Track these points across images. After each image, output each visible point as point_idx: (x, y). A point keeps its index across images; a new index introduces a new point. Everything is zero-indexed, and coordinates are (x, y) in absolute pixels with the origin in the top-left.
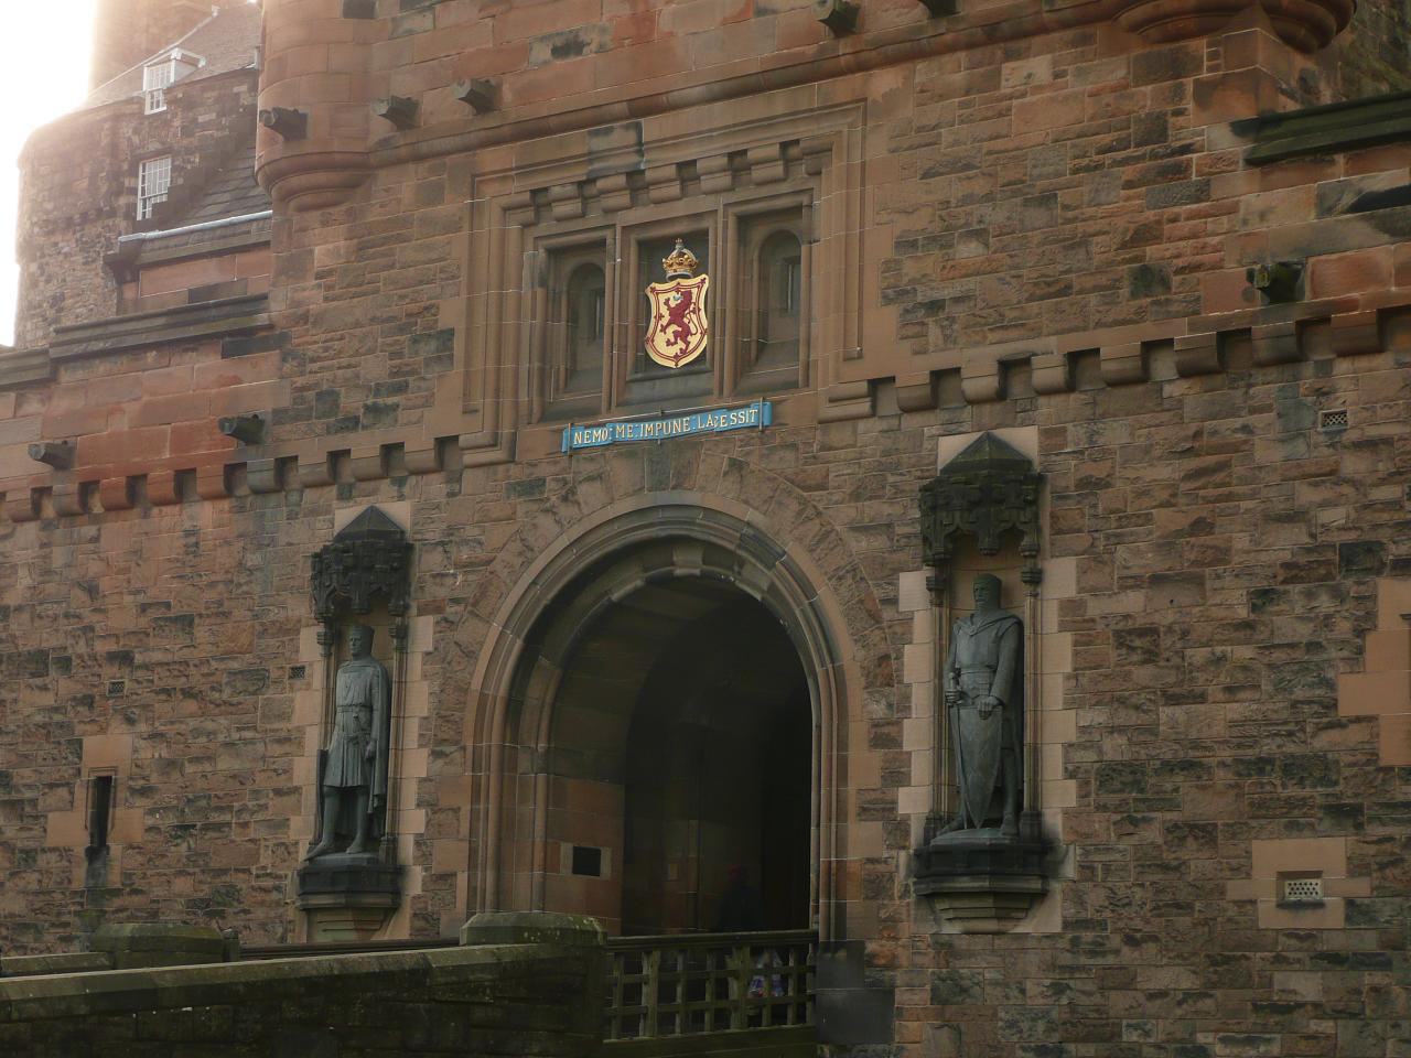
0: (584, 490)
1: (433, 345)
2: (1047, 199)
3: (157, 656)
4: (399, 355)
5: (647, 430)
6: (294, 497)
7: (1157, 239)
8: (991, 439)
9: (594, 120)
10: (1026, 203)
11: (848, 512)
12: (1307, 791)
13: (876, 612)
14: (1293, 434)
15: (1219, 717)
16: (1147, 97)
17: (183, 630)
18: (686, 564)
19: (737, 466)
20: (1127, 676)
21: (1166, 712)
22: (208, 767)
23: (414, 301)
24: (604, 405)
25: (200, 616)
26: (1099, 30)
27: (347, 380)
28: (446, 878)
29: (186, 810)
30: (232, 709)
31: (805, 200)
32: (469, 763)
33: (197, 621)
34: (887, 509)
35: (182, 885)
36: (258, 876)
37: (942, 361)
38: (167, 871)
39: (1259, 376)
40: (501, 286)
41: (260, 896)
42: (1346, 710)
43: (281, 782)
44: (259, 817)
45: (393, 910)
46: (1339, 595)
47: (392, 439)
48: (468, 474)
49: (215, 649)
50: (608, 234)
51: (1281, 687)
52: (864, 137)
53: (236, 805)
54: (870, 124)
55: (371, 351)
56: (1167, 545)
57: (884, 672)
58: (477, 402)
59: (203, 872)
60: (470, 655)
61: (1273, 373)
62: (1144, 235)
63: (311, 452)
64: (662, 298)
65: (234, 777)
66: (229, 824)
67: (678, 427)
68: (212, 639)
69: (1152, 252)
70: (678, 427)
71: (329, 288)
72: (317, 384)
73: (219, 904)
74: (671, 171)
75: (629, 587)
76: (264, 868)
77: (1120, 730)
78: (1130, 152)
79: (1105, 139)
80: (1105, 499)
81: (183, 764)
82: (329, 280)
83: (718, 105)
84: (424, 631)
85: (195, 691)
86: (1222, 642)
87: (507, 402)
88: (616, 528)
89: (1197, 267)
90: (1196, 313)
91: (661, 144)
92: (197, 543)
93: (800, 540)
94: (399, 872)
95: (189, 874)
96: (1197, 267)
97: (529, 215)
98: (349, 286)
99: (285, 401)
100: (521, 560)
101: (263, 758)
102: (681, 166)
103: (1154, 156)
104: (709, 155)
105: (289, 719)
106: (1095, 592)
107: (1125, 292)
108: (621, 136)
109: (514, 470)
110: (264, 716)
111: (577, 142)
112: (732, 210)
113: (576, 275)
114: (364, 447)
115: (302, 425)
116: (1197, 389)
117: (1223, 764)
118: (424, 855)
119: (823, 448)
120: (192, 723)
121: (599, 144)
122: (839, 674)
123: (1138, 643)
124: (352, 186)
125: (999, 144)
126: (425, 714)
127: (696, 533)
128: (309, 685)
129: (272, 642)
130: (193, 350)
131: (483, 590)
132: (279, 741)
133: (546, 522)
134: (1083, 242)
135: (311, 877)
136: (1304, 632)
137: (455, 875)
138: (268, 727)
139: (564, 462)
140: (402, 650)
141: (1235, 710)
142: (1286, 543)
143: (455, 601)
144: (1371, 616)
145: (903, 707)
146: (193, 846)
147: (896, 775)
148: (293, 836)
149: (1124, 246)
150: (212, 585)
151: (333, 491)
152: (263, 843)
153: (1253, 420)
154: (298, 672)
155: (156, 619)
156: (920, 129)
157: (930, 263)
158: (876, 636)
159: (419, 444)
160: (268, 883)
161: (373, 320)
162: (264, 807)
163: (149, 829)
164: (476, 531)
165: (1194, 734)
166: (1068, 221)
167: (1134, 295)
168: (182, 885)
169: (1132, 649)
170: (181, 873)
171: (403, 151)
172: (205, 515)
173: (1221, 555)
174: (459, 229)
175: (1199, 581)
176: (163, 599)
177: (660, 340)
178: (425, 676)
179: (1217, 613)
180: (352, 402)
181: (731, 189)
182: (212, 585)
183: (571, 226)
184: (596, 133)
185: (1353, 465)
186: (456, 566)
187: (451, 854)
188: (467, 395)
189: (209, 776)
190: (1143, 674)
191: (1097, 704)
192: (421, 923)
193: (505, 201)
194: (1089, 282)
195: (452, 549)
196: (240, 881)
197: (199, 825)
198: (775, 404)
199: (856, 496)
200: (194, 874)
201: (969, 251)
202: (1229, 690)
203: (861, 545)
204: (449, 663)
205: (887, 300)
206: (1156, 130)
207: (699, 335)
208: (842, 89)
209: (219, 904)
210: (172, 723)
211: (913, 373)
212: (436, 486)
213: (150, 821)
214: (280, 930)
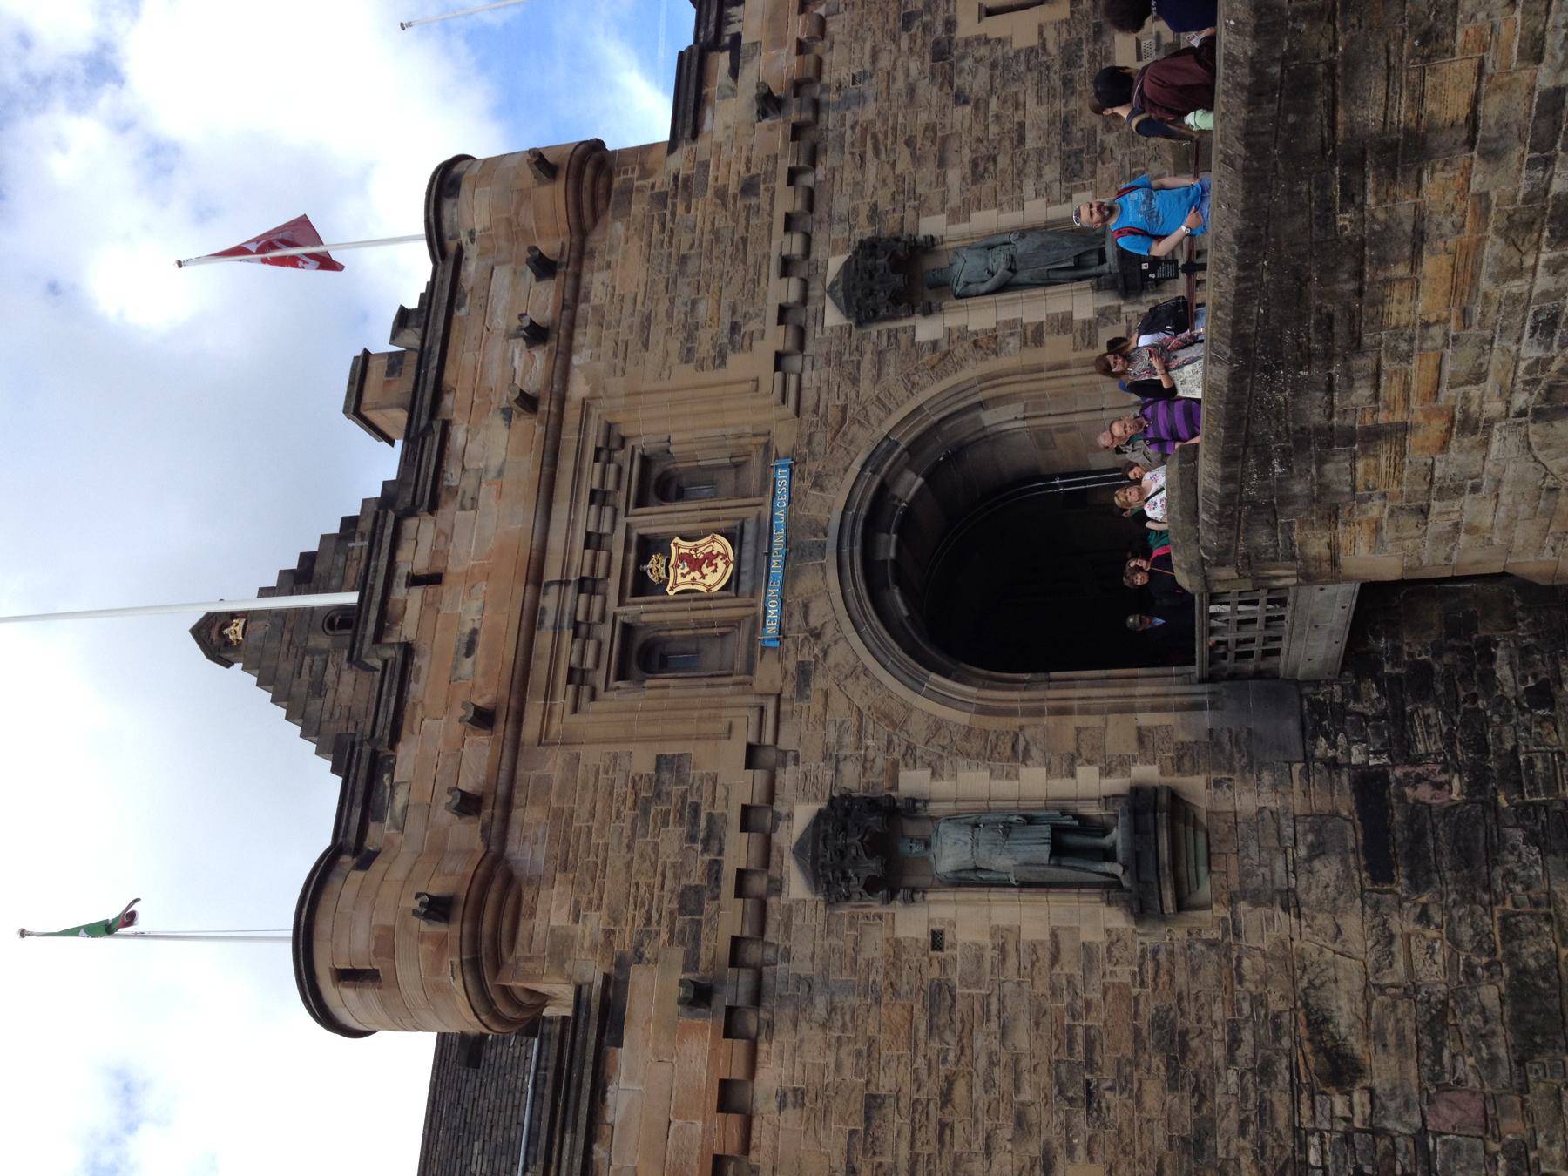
0: (815, 622)
1: (666, 776)
2: (683, 260)
3: (904, 1151)
4: (668, 812)
5: (776, 567)
6: (770, 953)
7: (725, 187)
8: (831, 291)
9: (532, 619)
10: (683, 273)
11: (866, 385)
12: (1085, 54)
13: (942, 356)
14: (861, 98)
15: (1036, 113)
16: (639, 207)
17: (880, 1107)
18: (888, 545)
19: (818, 484)
20: (1004, 172)
21: (1030, 143)
22: (1025, 1063)
23: (624, 803)
24: (750, 611)
25: (868, 1082)
26: (589, 245)
27: (676, 876)
28: (1142, 736)
29: (1070, 1094)
30: (968, 1027)
31: (638, 451)
32: (1036, 720)
33: (872, 1089)
34: (868, 356)
35: (1151, 1101)
36: (1142, 984)
37: (772, 314)
38: (1137, 1124)
39: (822, 124)
40: (631, 710)
41: (1164, 978)
42: (1034, 41)
43: (1045, 955)
44: (1079, 984)
45: (1174, 795)
46: (963, 57)
47: (735, 817)
48: (782, 745)
49: (904, 1060)
50: (619, 619)
51: (1018, 78)
52: (608, 397)
53: (1067, 1021)
54: (601, 393)
55: (655, 848)
56: (917, 159)
57: (987, 344)
58: (721, 727)
59: (1137, 1066)
60: (938, 726)
61: (823, 116)
62: (721, 194)
63: (729, 918)
64: (680, 580)
65: (1037, 1025)
66: (1087, 1029)
67: (779, 539)
68: (893, 1065)
69: (733, 189)
70: (779, 539)
71: (590, 902)
72: (671, 913)
73: (1172, 1042)
74: (589, 553)
75: (899, 599)
76: (1134, 974)
77: (1039, 169)
78: (668, 213)
79: (656, 226)
80: (884, 204)
81: (1022, 1104)
82: (583, 904)
83: (554, 516)
84: (913, 781)
85: (944, 1085)
86: (986, 118)
87: (730, 700)
88: (850, 590)
89: (749, 160)
90: (776, 156)
91: (566, 566)
92: (795, 1090)
93: (881, 422)
94: (1137, 792)
95: (1140, 1088)
96: (749, 160)
97: (586, 690)
98: (593, 880)
99: (678, 954)
100: (862, 677)
101: (1019, 984)
102: (587, 546)
103: (675, 196)
104: (586, 518)
105: (982, 948)
106: (944, 202)
107: (753, 201)
108: (549, 602)
109: (786, 695)
110: (977, 984)
111: (544, 640)
112: (631, 511)
113: (643, 656)
114: (738, 850)
115: (705, 930)
116: (823, 159)
117: (1065, 105)
118: (1121, 764)
119: (816, 411)
120: (978, 1091)
121: (549, 621)
122: (985, 378)
123: (981, 168)
124: (510, 879)
125: (640, 298)
126: (987, 773)
127: (863, 512)
128: (953, 924)
129: (904, 973)
130: (605, 1092)
131: (885, 715)
132: (1004, 959)
133: (837, 654)
134: (716, 233)
135: (1142, 909)
136: (984, 73)
137: (1139, 728)
138: (988, 977)
139: (789, 642)
140: (926, 802)
141: (1031, 102)
142: (929, 93)
143: (890, 742)
144: (978, 38)
145: (1012, 325)
146: (1109, 1083)
147: (1064, 323)
148: (1099, 938)
149: (725, 205)
150: (838, 1067)
151: (773, 900)
152: (1108, 979)
153: (848, 123)
154: (937, 941)
155: (865, 1151)
156: (615, 355)
157: (704, 335)
158: (959, 352)
159: (743, 786)
160: (1150, 965)
161: (629, 848)
162: (1070, 979)
163: (1090, 1152)
164: (832, 729)
165: (1046, 125)
166: (700, 245)
167: (757, 195)
168: (1152, 1094)
169: (986, 169)
170: (1139, 1102)
171: (498, 812)
172: (771, 1077)
173: (930, 128)
174: (578, 757)
175: (945, 139)
176: (843, 1140)
177: (712, 579)
178: (954, 776)
179: (967, 123)
180: (696, 878)
181: (615, 511)
182: (838, 1067)
183: (606, 648)
184: (542, 622)
185: (885, 62)
186: (858, 748)
187: (1118, 733)
188: (716, 737)
189: (1034, 1062)
190: (1003, 161)
191: (1020, 188)
192: (1187, 763)
193: (568, 709)
194: (743, 222)
195: (845, 752)
196: (1147, 1011)
197: (1087, 1076)
198: (777, 457)
199: (855, 381)
200: (1140, 1081)
201: (704, 309)
202: (1017, 108)
203: (892, 370)
204: (944, 748)
205: (723, 363)
206: (661, 199)
207: (716, 545)
208: (572, 417)
209: (1172, 1042)
210: (976, 1121)
211: (777, 338)
212: (788, 777)
213: (1081, 1152)
214: (1199, 947)
